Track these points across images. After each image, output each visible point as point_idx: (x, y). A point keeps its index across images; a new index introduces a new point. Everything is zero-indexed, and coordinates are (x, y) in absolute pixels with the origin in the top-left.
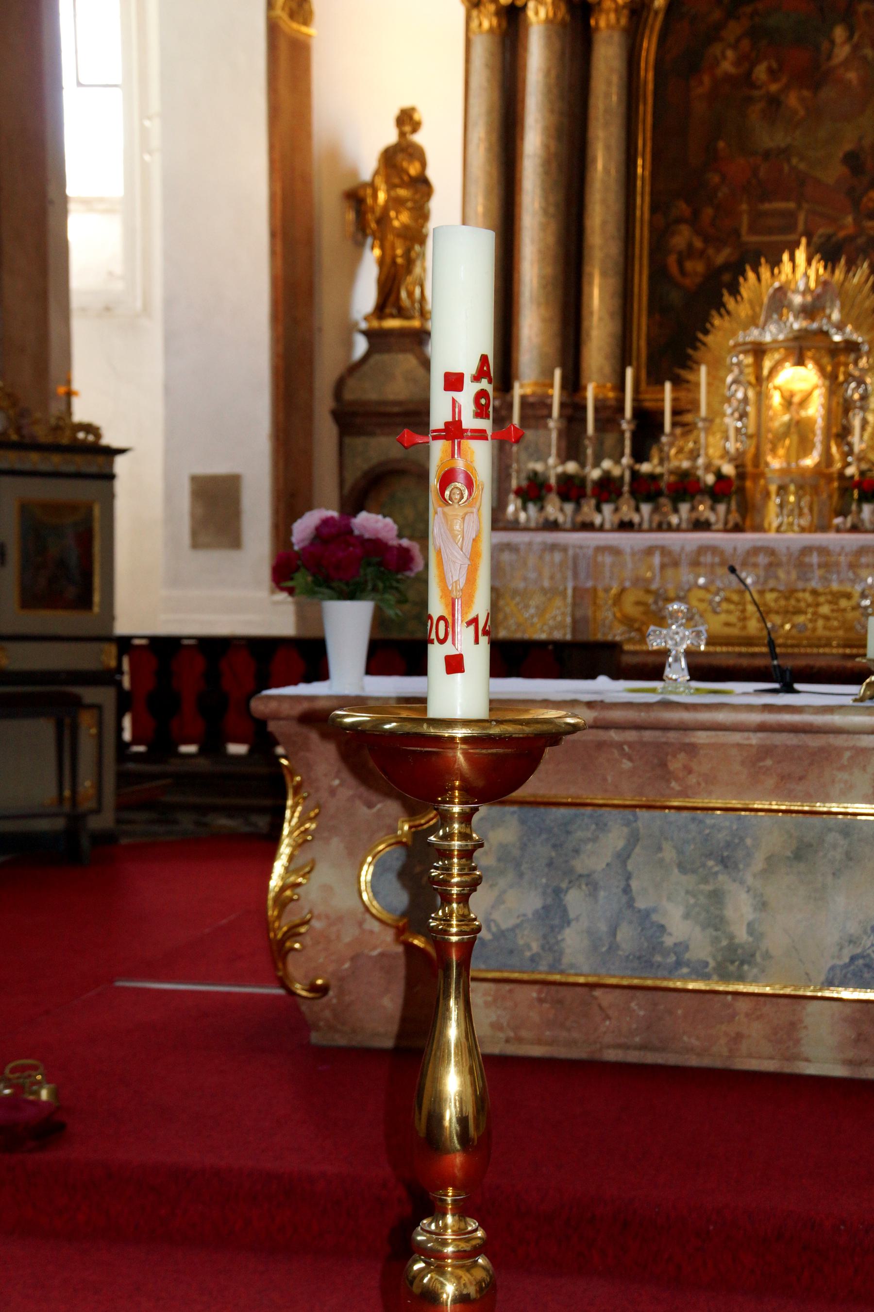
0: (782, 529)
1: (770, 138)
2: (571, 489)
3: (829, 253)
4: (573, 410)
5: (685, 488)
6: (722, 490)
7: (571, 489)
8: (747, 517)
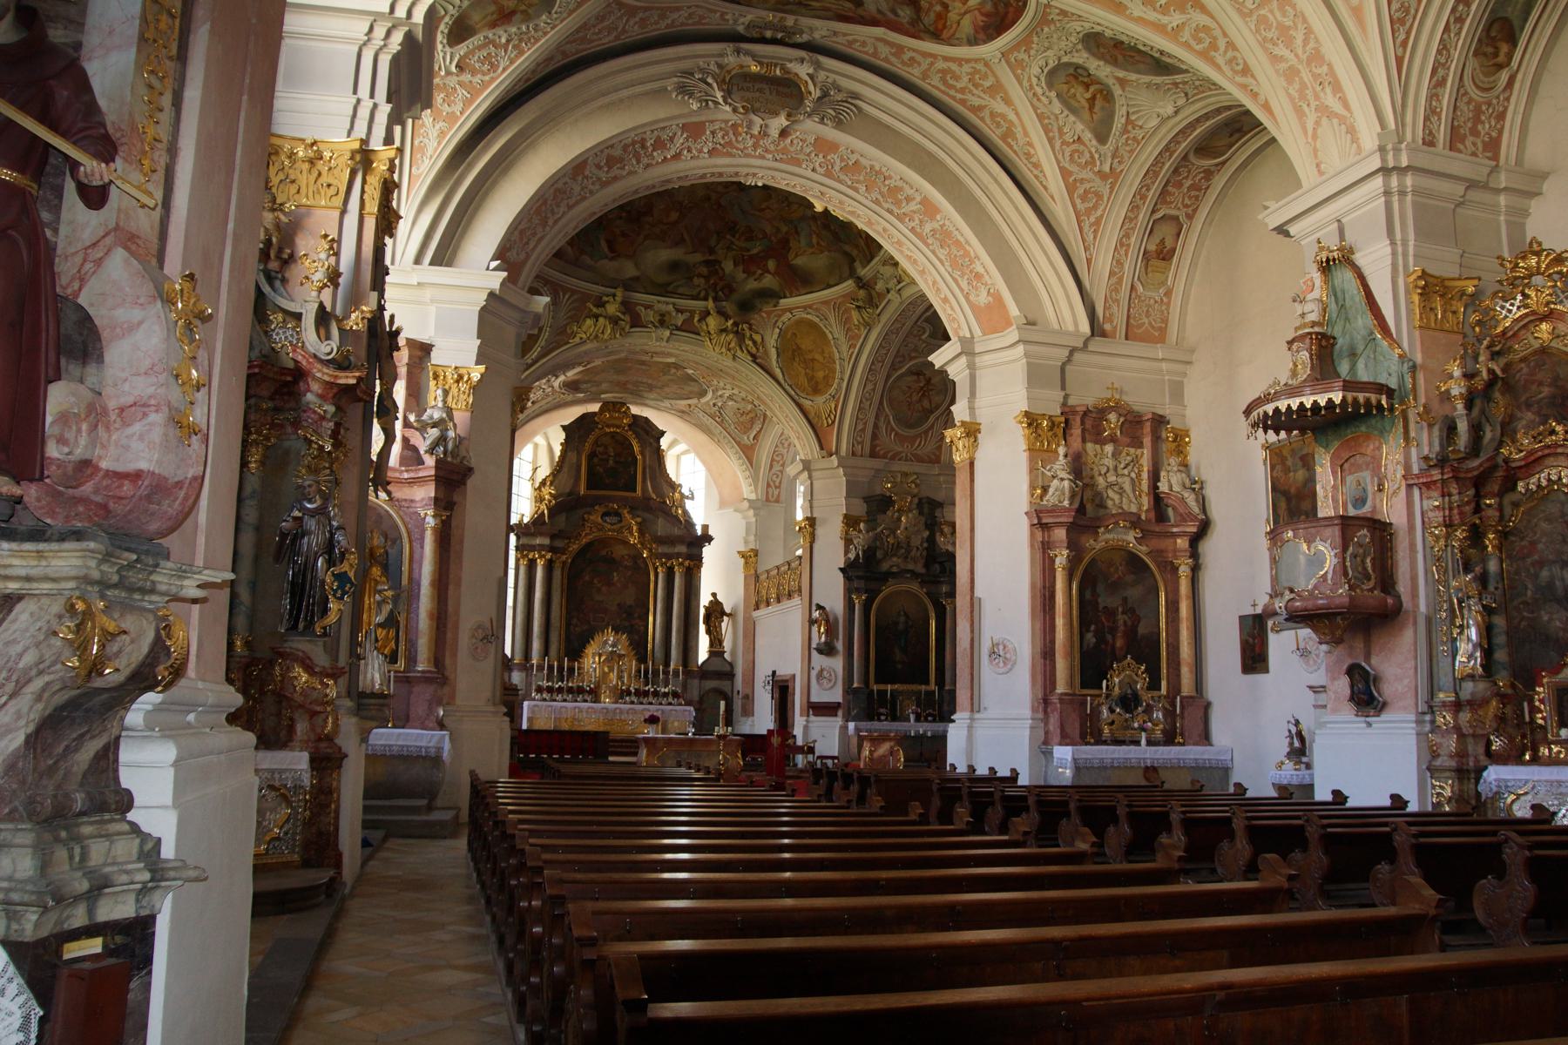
0: (607, 701)
1: (598, 598)
2: (550, 690)
3: (616, 630)
4: (551, 668)
5: (580, 690)
6: (591, 692)
7: (550, 690)
8: (597, 700)
